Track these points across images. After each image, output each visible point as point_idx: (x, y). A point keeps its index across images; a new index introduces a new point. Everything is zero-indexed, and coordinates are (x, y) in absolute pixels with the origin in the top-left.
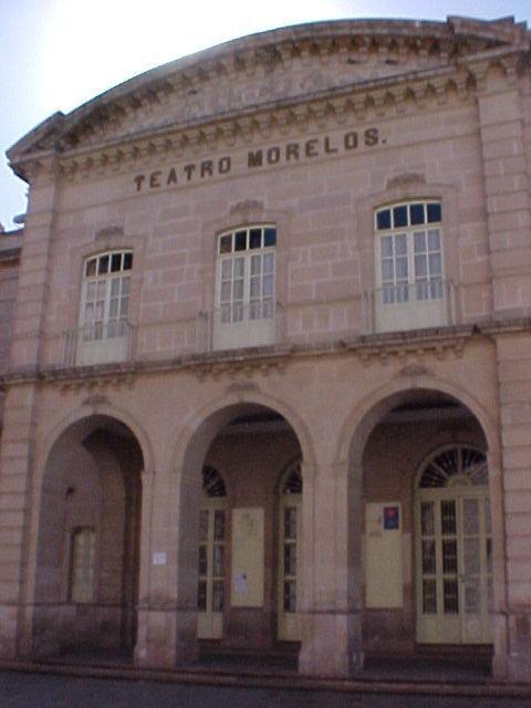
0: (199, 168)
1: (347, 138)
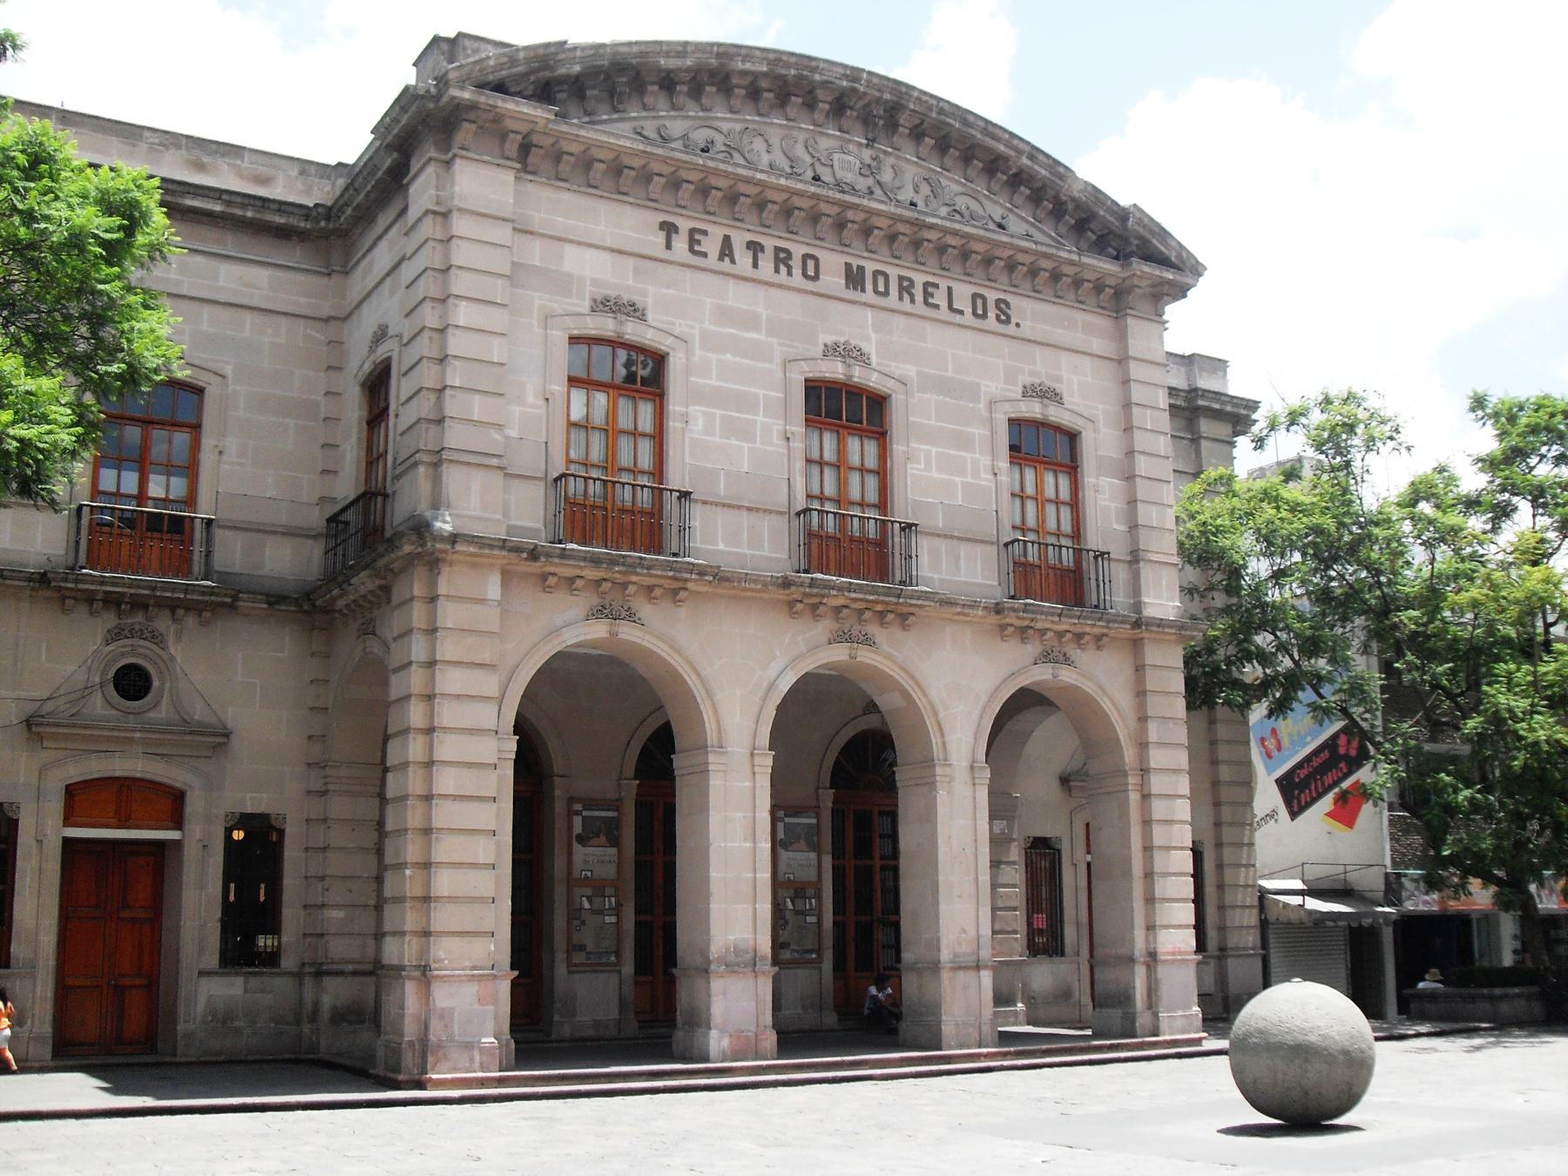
0: (769, 252)
1: (975, 296)
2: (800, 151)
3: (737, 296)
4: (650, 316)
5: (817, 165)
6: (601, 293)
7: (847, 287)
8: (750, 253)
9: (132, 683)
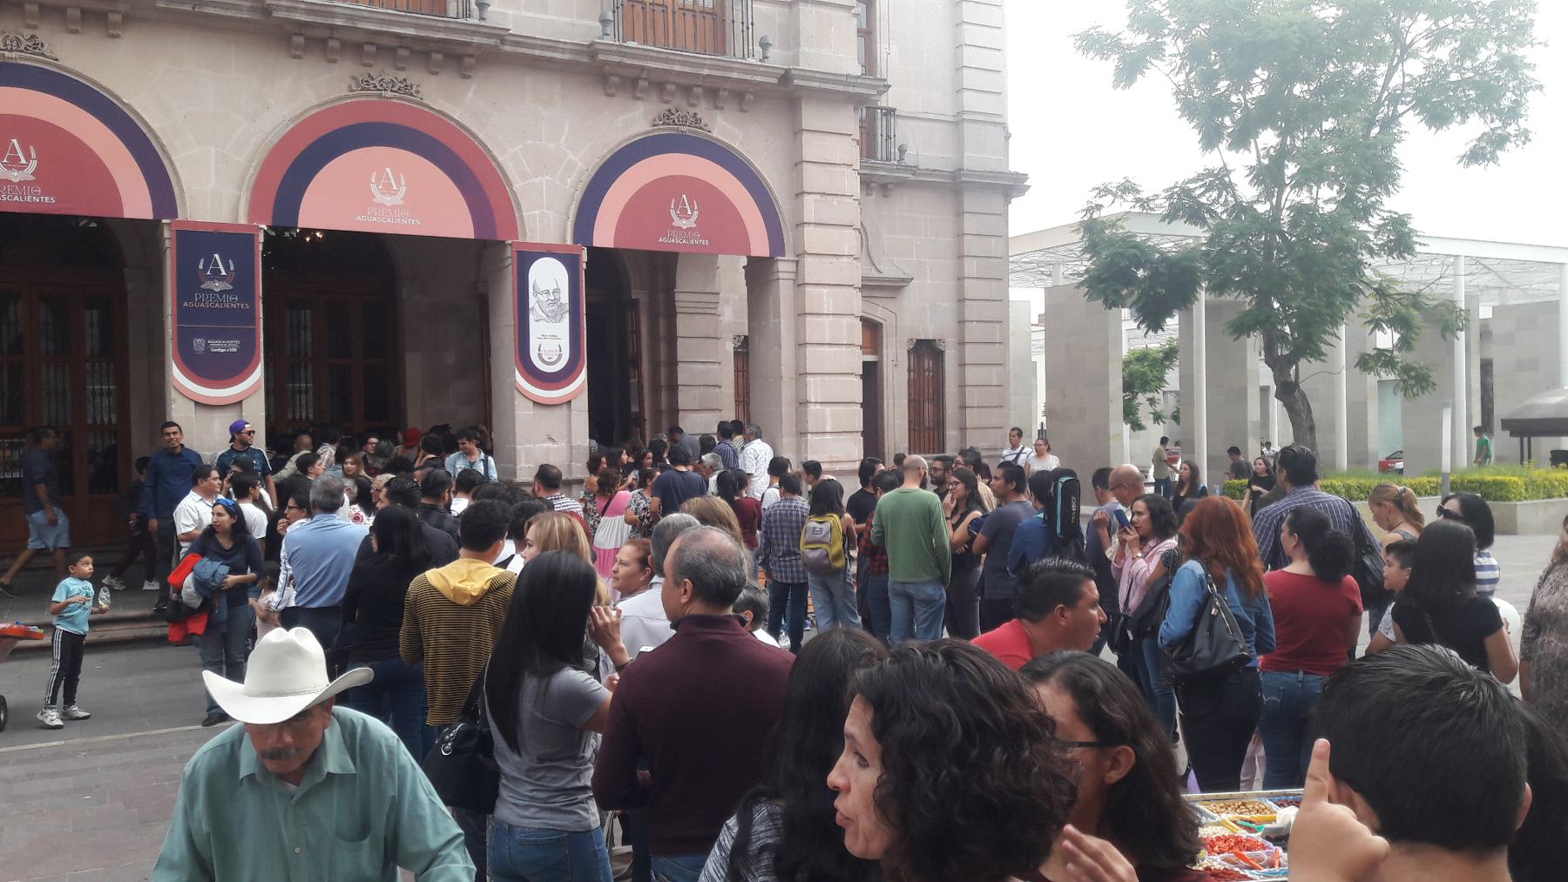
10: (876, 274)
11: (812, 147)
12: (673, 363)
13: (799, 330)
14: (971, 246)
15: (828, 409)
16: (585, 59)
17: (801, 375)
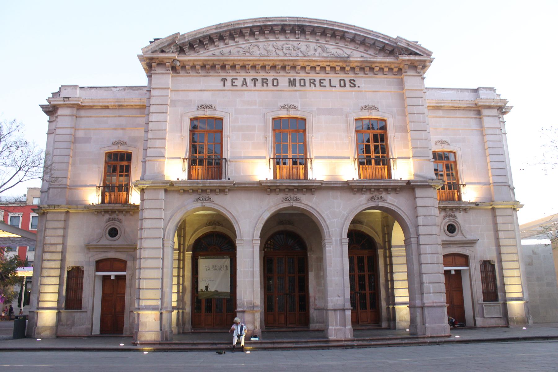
1: (340, 80)
2: (271, 48)
3: (247, 96)
4: (217, 108)
5: (277, 51)
6: (200, 104)
7: (289, 86)
8: (253, 82)
9: (113, 233)
10: (465, 239)
11: (419, 202)
12: (392, 273)
13: (419, 260)
14: (500, 227)
15: (431, 285)
16: (346, 185)
17: (421, 274)
